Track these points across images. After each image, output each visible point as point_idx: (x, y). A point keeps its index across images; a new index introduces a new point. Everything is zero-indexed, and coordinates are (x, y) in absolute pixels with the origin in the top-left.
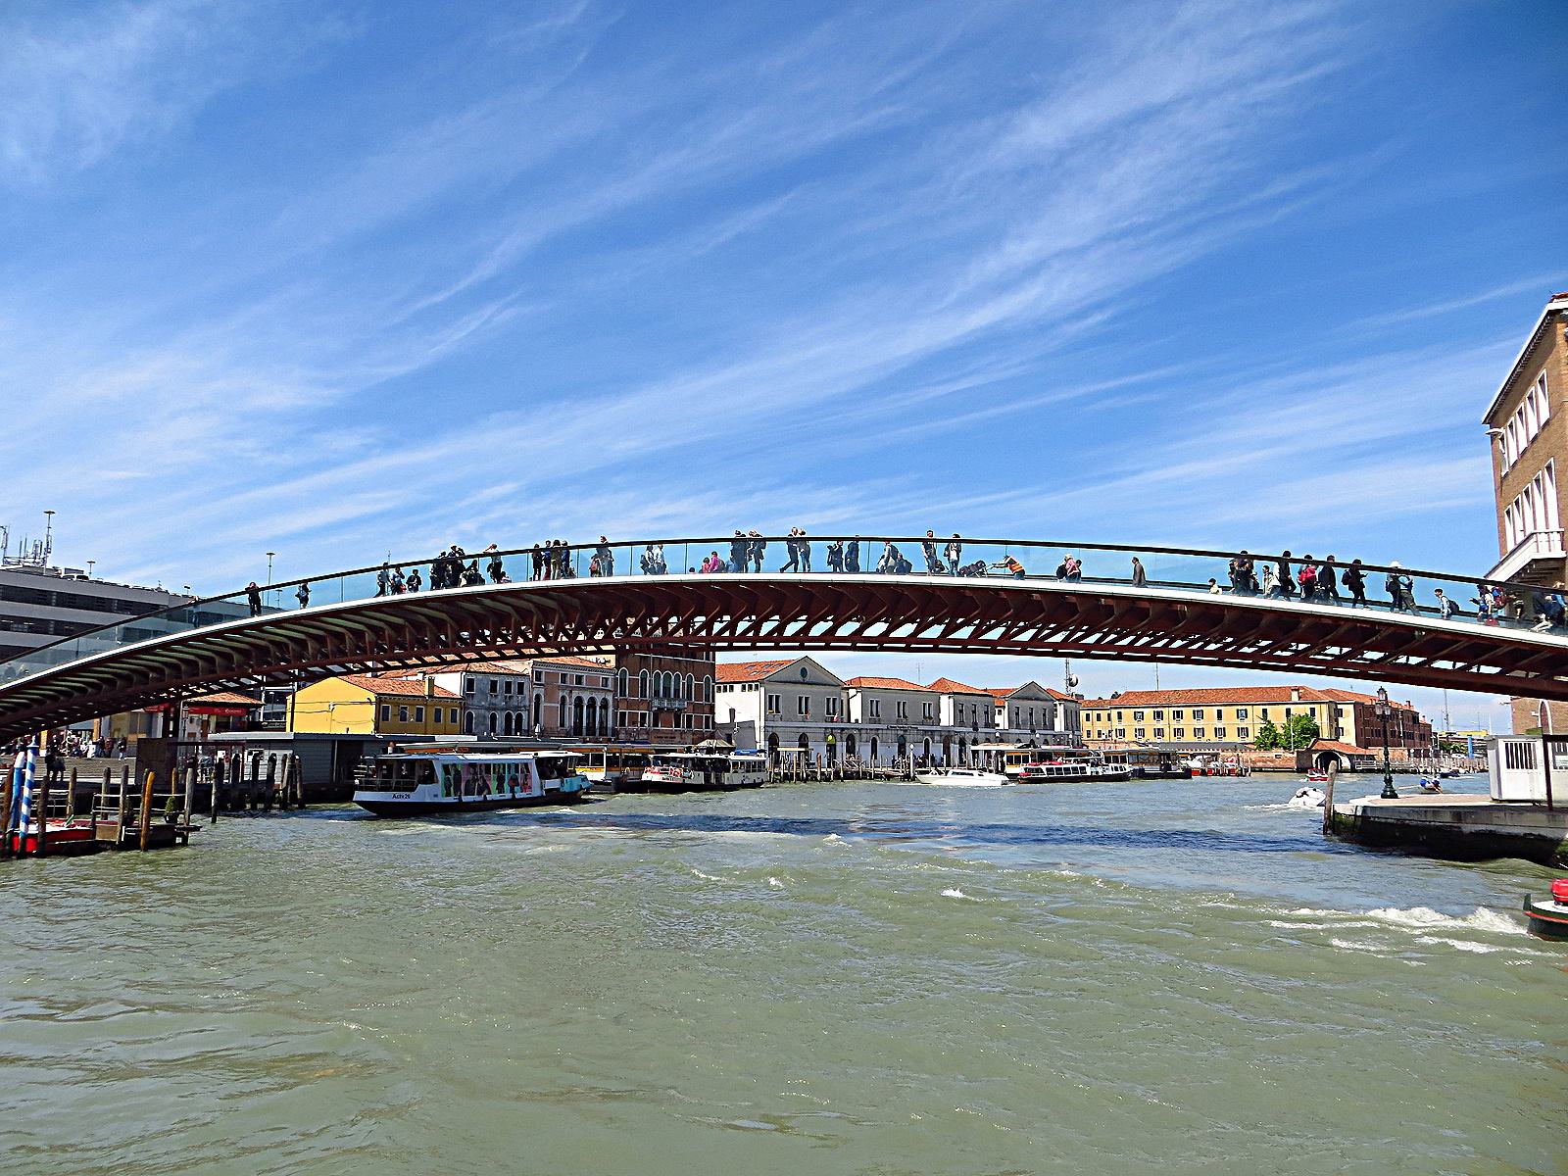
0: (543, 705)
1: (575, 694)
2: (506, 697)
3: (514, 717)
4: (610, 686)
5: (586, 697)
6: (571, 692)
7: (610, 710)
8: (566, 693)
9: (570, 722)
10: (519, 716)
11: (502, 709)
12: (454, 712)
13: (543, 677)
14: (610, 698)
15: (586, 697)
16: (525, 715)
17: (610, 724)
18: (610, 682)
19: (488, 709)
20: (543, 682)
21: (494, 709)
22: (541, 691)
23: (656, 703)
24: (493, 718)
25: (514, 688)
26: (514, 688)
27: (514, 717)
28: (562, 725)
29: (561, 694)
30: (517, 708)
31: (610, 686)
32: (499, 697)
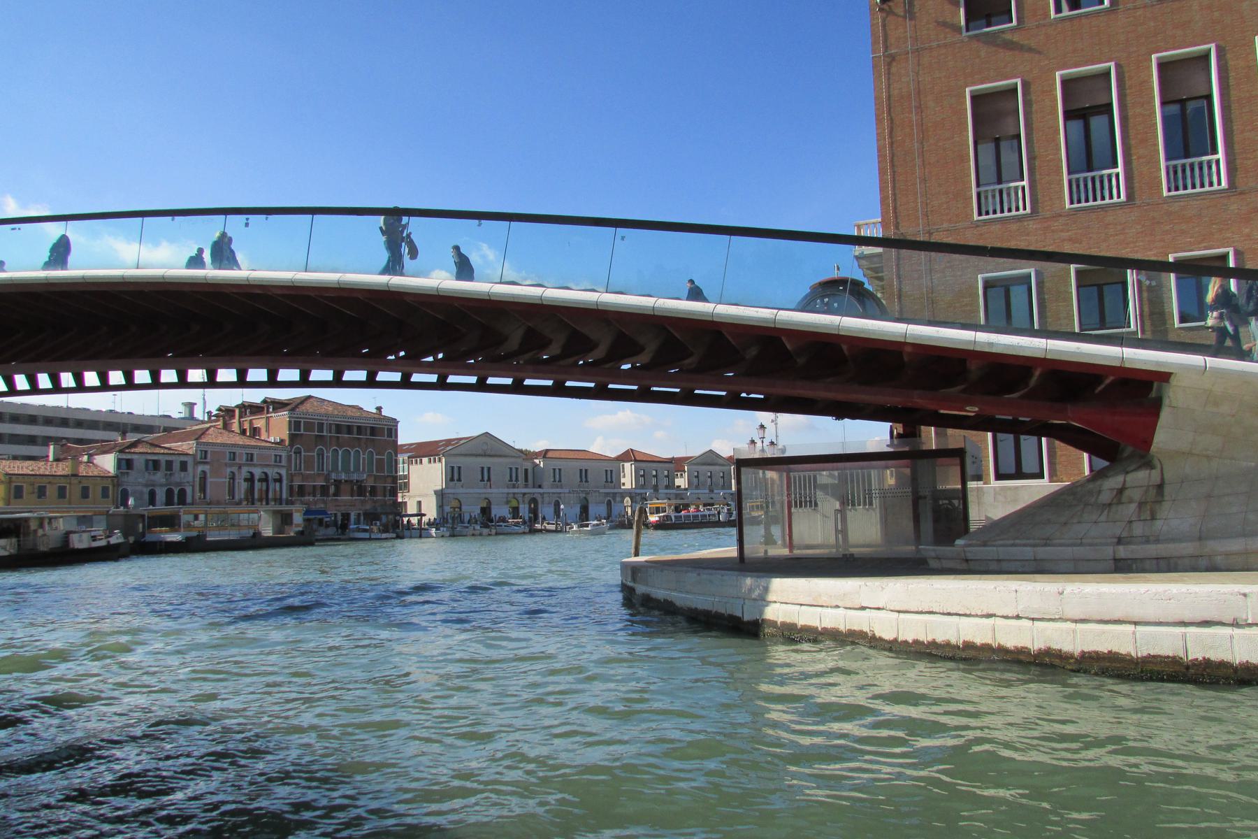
0: (209, 480)
1: (245, 470)
2: (166, 475)
3: (176, 492)
4: (284, 463)
5: (258, 472)
6: (240, 468)
7: (285, 482)
8: (235, 469)
11: (161, 485)
12: (105, 490)
13: (209, 456)
14: (283, 472)
15: (258, 472)
16: (189, 490)
17: (284, 496)
19: (146, 485)
20: (208, 460)
22: (207, 468)
23: (333, 476)
25: (176, 466)
26: (176, 466)
27: (176, 492)
29: (229, 470)
31: (284, 463)
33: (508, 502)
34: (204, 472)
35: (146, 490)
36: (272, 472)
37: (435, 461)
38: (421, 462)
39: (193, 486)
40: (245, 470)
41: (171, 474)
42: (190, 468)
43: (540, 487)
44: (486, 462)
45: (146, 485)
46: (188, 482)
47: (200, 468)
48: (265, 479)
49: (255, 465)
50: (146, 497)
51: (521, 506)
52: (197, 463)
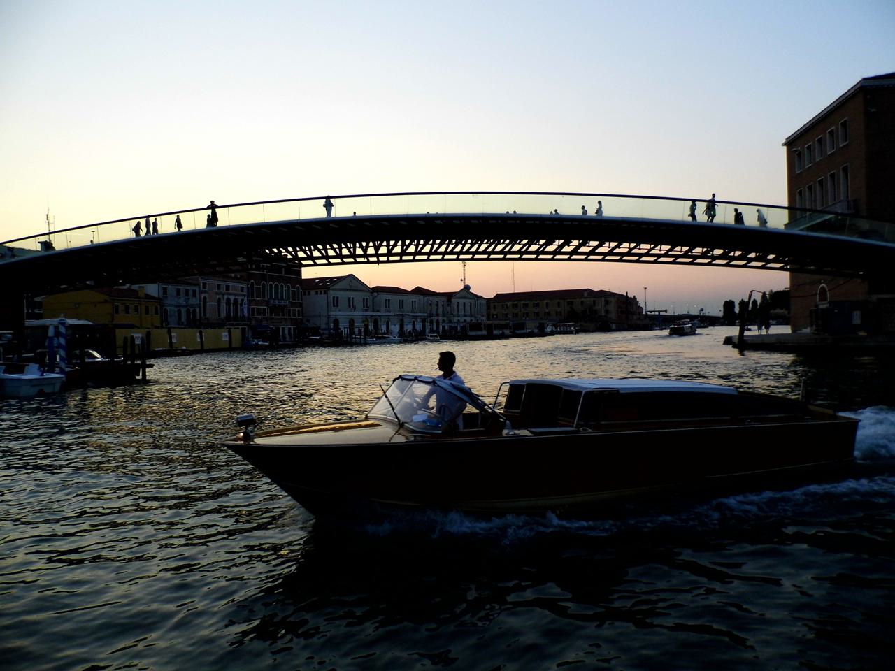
1: (226, 297)
5: (232, 298)
8: (220, 296)
9: (223, 315)
10: (195, 311)
11: (184, 306)
12: (156, 308)
15: (232, 298)
18: (245, 290)
19: (176, 306)
21: (179, 306)
22: (206, 295)
23: (272, 301)
24: (179, 312)
25: (191, 293)
26: (191, 293)
28: (219, 315)
29: (218, 297)
30: (192, 306)
32: (182, 299)
33: (363, 321)
34: (205, 298)
35: (176, 309)
36: (240, 298)
37: (321, 293)
38: (309, 294)
39: (200, 307)
40: (226, 297)
41: (188, 299)
42: (198, 296)
43: (378, 311)
44: (351, 294)
45: (176, 306)
46: (197, 304)
47: (203, 295)
48: (236, 300)
49: (231, 294)
50: (176, 314)
51: (370, 324)
52: (201, 293)
